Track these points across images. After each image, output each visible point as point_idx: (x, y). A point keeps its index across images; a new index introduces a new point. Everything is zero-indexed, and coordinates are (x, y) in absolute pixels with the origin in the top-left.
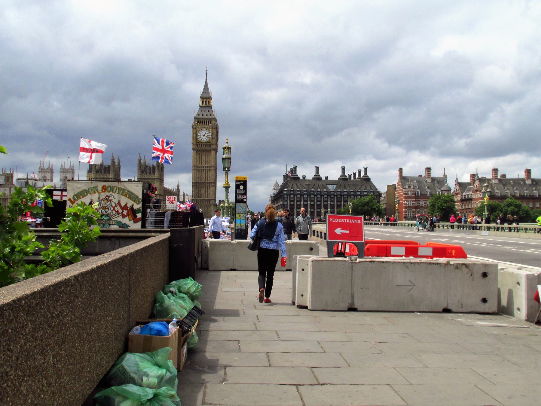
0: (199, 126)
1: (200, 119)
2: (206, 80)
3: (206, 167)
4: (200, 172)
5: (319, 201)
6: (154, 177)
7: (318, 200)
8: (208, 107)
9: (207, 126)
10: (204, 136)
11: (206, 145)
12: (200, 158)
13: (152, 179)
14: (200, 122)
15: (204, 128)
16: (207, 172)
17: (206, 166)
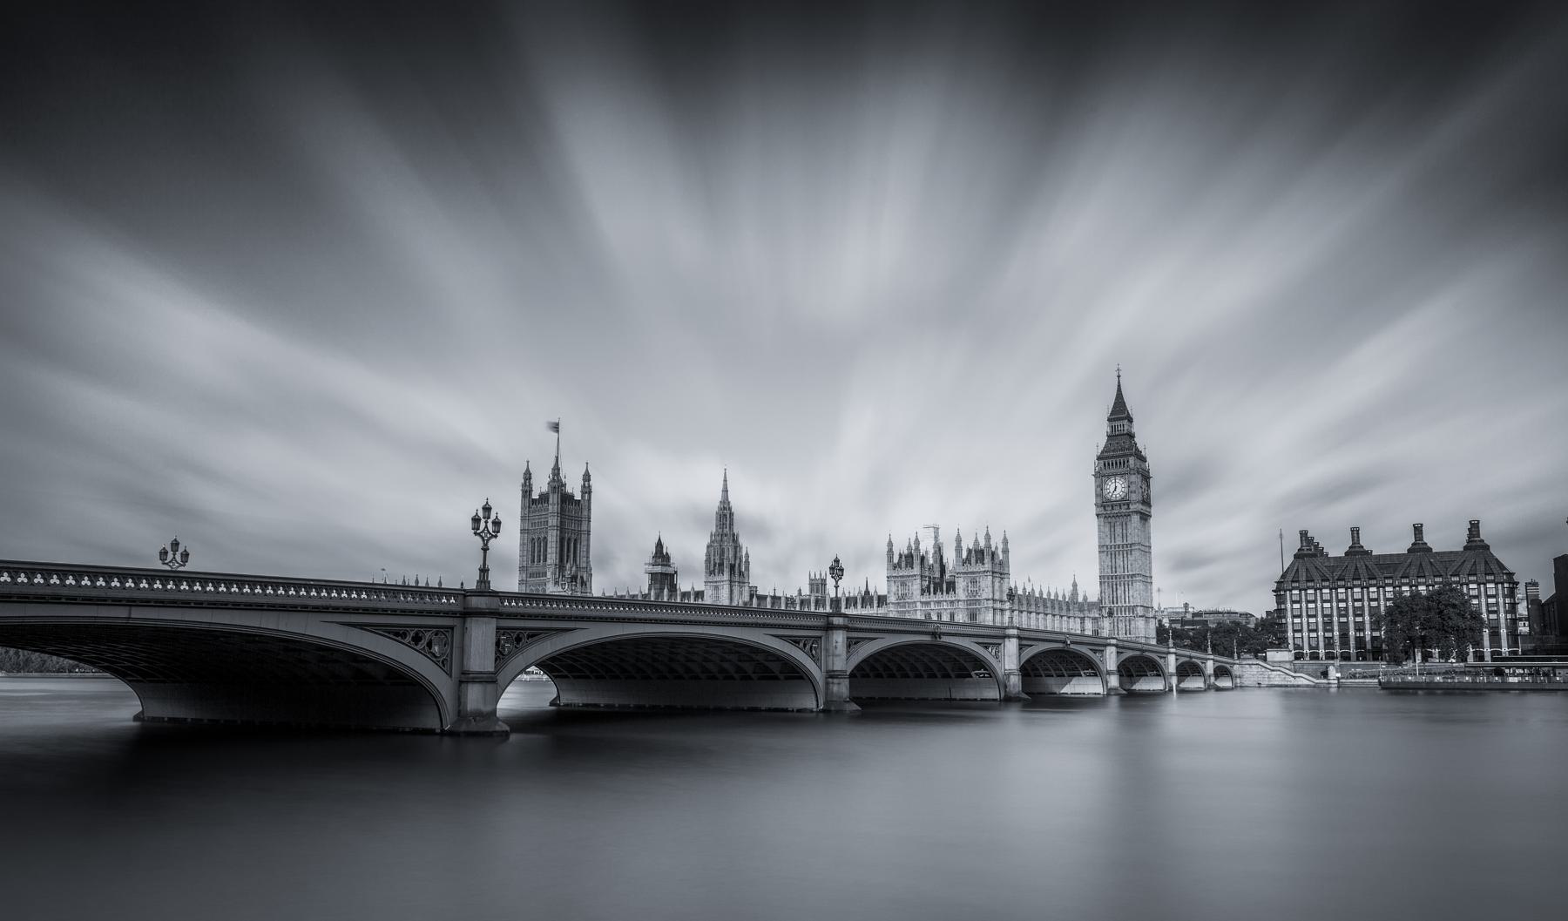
0: (1108, 471)
1: (1107, 458)
2: (1119, 386)
3: (1123, 547)
4: (1113, 556)
5: (1342, 601)
6: (982, 569)
7: (1355, 597)
8: (1123, 435)
9: (1120, 470)
10: (1117, 488)
11: (1120, 506)
12: (1112, 530)
13: (979, 573)
14: (1109, 464)
15: (1115, 475)
16: (1125, 555)
17: (1123, 545)
